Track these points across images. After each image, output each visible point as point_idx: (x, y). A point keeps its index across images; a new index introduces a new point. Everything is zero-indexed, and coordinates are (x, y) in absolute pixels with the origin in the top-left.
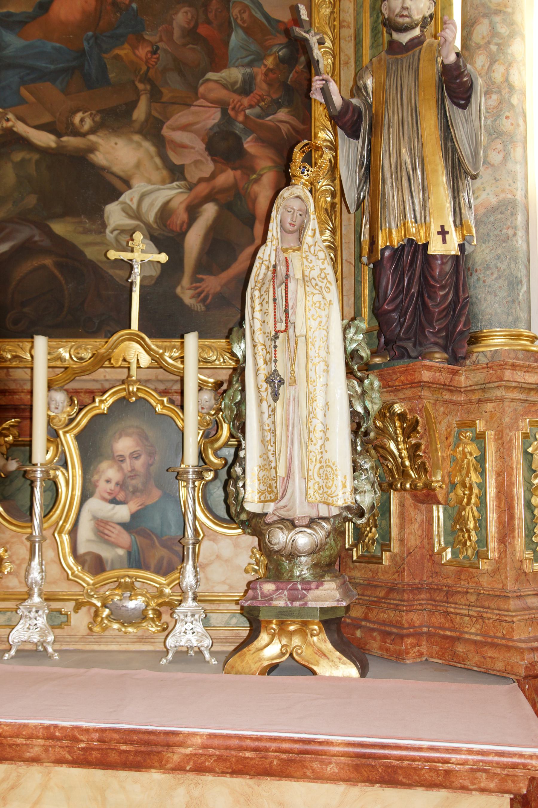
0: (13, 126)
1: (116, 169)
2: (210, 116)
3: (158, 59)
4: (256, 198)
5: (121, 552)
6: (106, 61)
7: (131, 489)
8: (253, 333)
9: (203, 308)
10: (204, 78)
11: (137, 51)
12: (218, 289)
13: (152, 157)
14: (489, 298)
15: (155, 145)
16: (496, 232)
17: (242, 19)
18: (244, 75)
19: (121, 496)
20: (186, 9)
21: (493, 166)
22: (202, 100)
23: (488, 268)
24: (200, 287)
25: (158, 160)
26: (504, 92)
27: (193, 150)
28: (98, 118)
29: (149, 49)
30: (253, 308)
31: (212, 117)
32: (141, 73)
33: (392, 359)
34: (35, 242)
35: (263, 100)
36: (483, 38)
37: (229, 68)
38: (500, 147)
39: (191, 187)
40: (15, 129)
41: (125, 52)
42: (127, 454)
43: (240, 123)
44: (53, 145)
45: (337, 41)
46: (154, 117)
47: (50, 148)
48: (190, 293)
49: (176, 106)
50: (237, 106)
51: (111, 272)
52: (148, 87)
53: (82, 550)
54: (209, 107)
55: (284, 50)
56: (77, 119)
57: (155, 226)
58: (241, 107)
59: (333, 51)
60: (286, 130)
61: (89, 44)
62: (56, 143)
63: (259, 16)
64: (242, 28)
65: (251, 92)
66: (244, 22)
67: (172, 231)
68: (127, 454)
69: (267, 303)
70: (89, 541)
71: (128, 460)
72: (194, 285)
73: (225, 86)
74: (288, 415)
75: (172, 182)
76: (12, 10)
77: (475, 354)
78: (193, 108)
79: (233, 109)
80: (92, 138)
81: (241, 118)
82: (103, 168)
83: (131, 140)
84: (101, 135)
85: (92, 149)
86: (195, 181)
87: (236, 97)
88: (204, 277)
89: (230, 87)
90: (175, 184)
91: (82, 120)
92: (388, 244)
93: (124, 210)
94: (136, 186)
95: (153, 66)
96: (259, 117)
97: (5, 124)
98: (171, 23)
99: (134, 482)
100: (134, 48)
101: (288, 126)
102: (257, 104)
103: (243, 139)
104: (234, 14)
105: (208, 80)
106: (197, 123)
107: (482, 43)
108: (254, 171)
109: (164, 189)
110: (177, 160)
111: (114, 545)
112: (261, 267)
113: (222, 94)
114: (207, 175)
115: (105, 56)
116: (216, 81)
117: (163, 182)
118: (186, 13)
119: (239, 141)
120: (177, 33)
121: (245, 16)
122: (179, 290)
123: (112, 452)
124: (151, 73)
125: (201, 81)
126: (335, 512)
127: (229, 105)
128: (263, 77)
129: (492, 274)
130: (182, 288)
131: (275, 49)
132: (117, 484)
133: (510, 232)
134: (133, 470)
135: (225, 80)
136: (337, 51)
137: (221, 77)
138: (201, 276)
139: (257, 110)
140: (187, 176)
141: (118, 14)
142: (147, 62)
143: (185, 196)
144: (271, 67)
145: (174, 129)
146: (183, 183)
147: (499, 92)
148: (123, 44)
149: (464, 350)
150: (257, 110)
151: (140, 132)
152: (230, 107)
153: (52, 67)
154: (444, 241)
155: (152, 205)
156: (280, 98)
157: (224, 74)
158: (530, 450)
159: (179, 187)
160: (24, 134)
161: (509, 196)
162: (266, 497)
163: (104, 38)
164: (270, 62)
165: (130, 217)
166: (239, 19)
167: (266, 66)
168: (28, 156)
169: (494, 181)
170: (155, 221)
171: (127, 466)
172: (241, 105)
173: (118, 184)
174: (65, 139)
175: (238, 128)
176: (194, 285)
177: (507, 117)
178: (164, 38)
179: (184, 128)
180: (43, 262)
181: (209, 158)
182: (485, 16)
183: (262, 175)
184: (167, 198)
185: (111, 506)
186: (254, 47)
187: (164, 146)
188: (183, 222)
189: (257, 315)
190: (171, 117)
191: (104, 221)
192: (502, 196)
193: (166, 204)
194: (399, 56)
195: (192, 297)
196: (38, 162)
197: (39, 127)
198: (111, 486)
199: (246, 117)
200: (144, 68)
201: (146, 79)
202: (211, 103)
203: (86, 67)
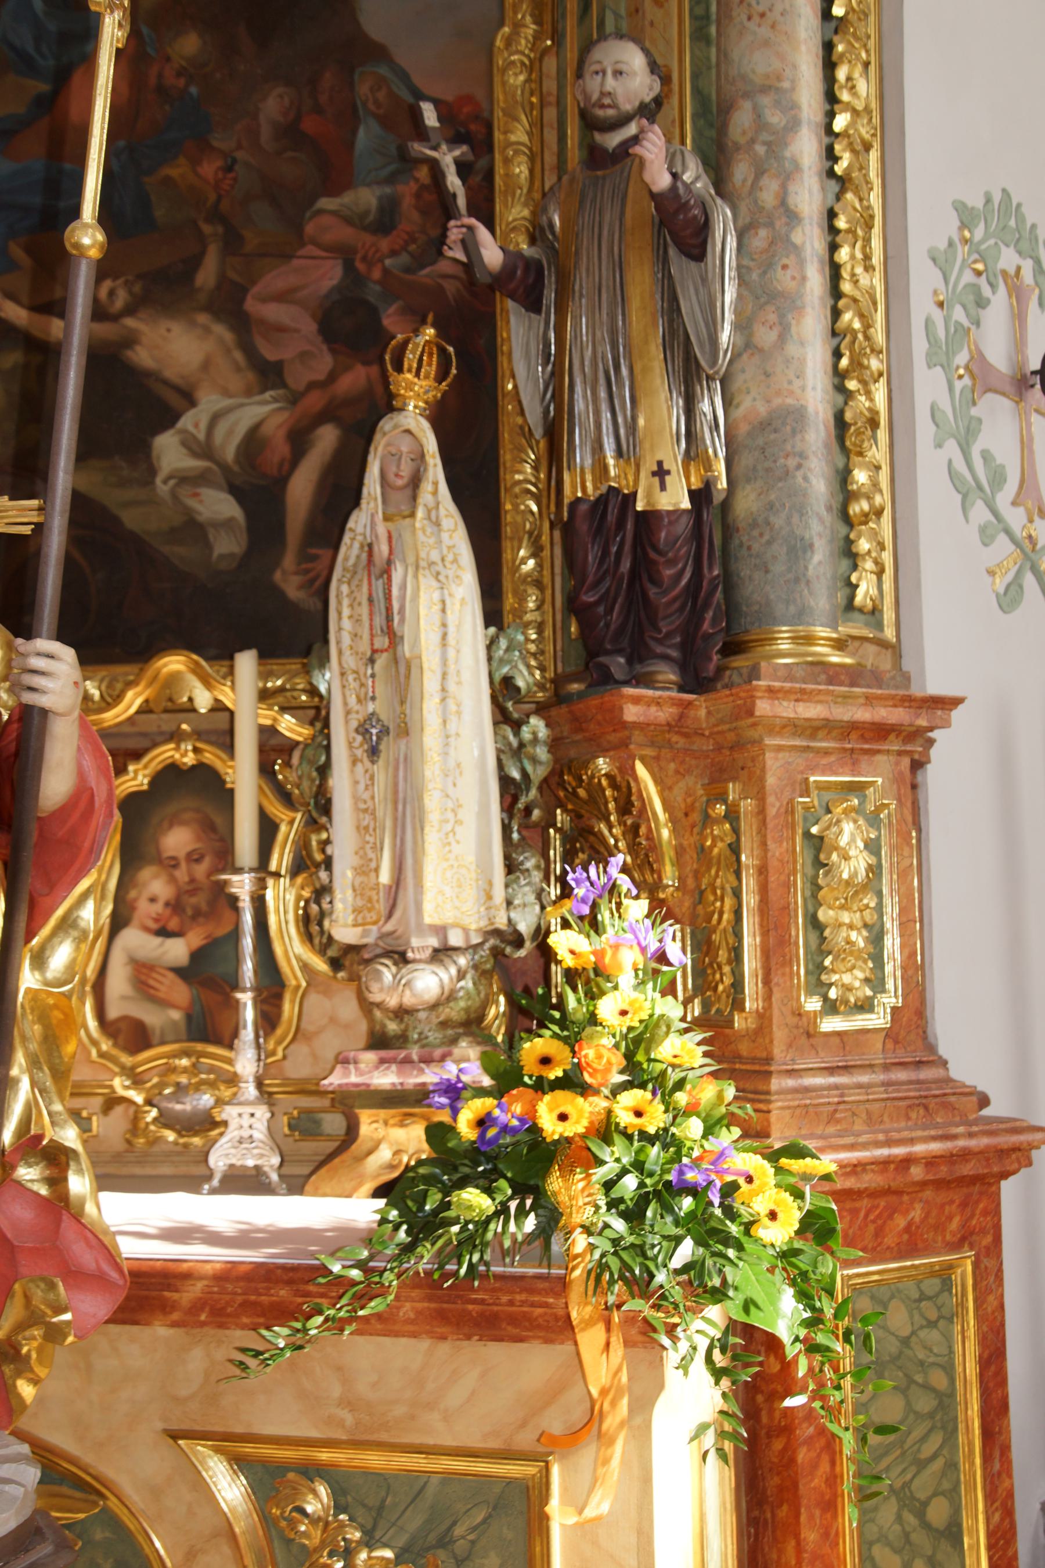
1: (169, 374)
3: (235, 179)
5: (176, 1015)
7: (189, 912)
8: (340, 653)
13: (228, 351)
14: (758, 575)
15: (233, 328)
16: (767, 464)
17: (376, 102)
18: (380, 199)
19: (173, 924)
20: (280, 90)
21: (761, 350)
23: (754, 525)
25: (238, 356)
26: (778, 224)
28: (137, 288)
29: (219, 163)
30: (339, 613)
33: (590, 686)
35: (414, 240)
36: (744, 133)
38: (772, 317)
39: (294, 399)
42: (181, 854)
51: (166, 549)
52: (220, 229)
53: (113, 1012)
54: (322, 258)
57: (236, 468)
58: (378, 255)
59: (530, 149)
68: (181, 854)
69: (360, 604)
70: (124, 998)
71: (183, 865)
72: (304, 566)
73: (348, 221)
74: (396, 785)
75: (262, 391)
77: (728, 673)
78: (295, 262)
79: (364, 259)
80: (129, 322)
81: (377, 274)
82: (148, 374)
85: (130, 341)
86: (301, 386)
87: (368, 238)
90: (267, 395)
91: (112, 293)
92: (579, 494)
93: (184, 444)
96: (408, 270)
99: (193, 900)
102: (404, 248)
105: (321, 212)
107: (742, 140)
110: (270, 353)
111: (164, 1003)
112: (351, 545)
113: (345, 234)
114: (321, 376)
117: (249, 393)
119: (374, 314)
121: (381, 95)
122: (278, 576)
123: (159, 852)
125: (308, 214)
126: (476, 940)
129: (761, 535)
132: (167, 904)
133: (792, 463)
134: (192, 880)
138: (314, 551)
139: (404, 259)
140: (290, 381)
141: (167, 107)
143: (285, 415)
145: (264, 300)
146: (281, 392)
147: (770, 225)
149: (712, 667)
152: (359, 256)
154: (663, 487)
155: (230, 432)
157: (347, 198)
158: (814, 830)
159: (275, 400)
161: (790, 401)
162: (364, 918)
165: (195, 454)
167: (417, 180)
169: (763, 377)
171: (182, 874)
173: (174, 400)
175: (373, 292)
176: (304, 566)
177: (785, 267)
179: (281, 297)
181: (324, 347)
182: (746, 95)
184: (256, 420)
185: (158, 940)
189: (346, 624)
192: (777, 401)
194: (599, 173)
195: (301, 587)
198: (158, 908)
199: (386, 271)
200: (212, 197)
201: (215, 215)
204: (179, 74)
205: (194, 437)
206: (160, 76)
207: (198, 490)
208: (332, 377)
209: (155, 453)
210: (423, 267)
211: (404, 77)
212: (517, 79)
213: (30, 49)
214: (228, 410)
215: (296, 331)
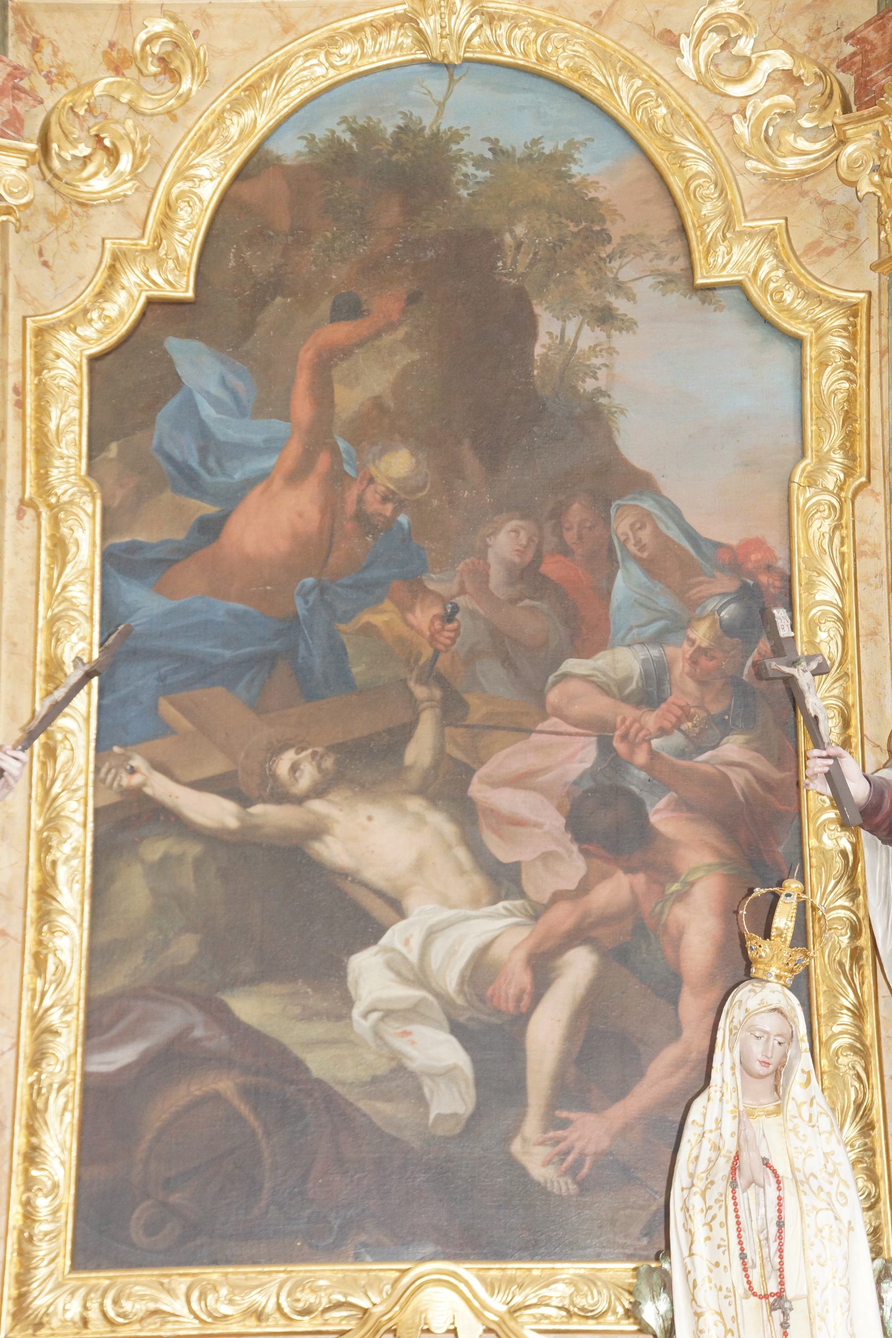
0: (144, 784)
1: (371, 875)
2: (573, 756)
3: (457, 631)
4: (681, 935)
6: (344, 638)
9: (573, 1188)
10: (559, 672)
11: (410, 617)
12: (605, 1144)
13: (449, 847)
15: (454, 819)
17: (638, 542)
18: (644, 662)
20: (514, 523)
22: (555, 720)
24: (565, 1139)
25: (462, 854)
27: (537, 830)
28: (328, 763)
29: (437, 610)
31: (578, 757)
32: (422, 662)
34: (197, 1041)
35: (689, 717)
37: (613, 647)
39: (536, 913)
40: (148, 790)
41: (385, 617)
43: (641, 768)
44: (232, 823)
45: (849, 588)
46: (451, 758)
47: (231, 832)
48: (542, 1152)
49: (500, 734)
50: (633, 731)
51: (362, 1105)
52: (438, 693)
54: (570, 734)
55: (732, 606)
56: (283, 765)
57: (460, 1001)
58: (641, 735)
59: (842, 610)
60: (742, 783)
61: (306, 602)
62: (240, 819)
63: (674, 533)
64: (638, 560)
65: (664, 700)
66: (642, 548)
67: (498, 1012)
72: (551, 1134)
73: (603, 689)
75: (494, 902)
76: (142, 537)
78: (535, 737)
79: (624, 737)
80: (317, 806)
81: (641, 757)
82: (344, 874)
83: (402, 810)
84: (337, 799)
86: (545, 898)
87: (629, 712)
88: (572, 1116)
89: (615, 690)
90: (501, 905)
91: (294, 768)
93: (390, 966)
94: (416, 912)
95: (446, 646)
96: (682, 754)
97: (127, 781)
98: (483, 553)
100: (405, 609)
101: (747, 774)
102: (677, 726)
103: (648, 803)
104: (620, 531)
105: (566, 676)
106: (545, 770)
108: (674, 876)
109: (478, 917)
110: (503, 853)
114: (571, 884)
115: (342, 627)
116: (585, 678)
117: (475, 903)
118: (516, 531)
120: (496, 576)
121: (645, 535)
122: (516, 1147)
124: (443, 663)
125: (551, 679)
127: (614, 729)
128: (687, 668)
130: (525, 1140)
131: (712, 605)
135: (605, 674)
136: (850, 608)
137: (594, 669)
138: (564, 1114)
139: (677, 739)
141: (369, 539)
142: (432, 639)
143: (524, 933)
144: (705, 644)
145: (496, 784)
146: (519, 903)
148: (380, 600)
150: (677, 739)
151: (421, 791)
152: (617, 733)
153: (228, 654)
155: (451, 953)
156: (726, 712)
159: (512, 914)
160: (168, 801)
163: (339, 589)
164: (701, 633)
165: (406, 981)
166: (632, 541)
167: (693, 642)
168: (176, 850)
170: (461, 991)
172: (641, 728)
173: (378, 909)
174: (258, 809)
178: (468, 586)
179: (519, 781)
180: (214, 1086)
181: (575, 848)
183: (692, 884)
184: (486, 938)
186: (665, 601)
187: (475, 822)
188: (522, 991)
190: (490, 755)
191: (347, 991)
193: (484, 950)
195: (547, 1163)
196: (198, 864)
197: (200, 785)
199: (653, 755)
202: (576, 726)
203: (302, 651)
204: (385, 499)
205: (405, 958)
206: (360, 500)
207: (409, 1028)
208: (584, 888)
209: (350, 978)
210: (701, 750)
211: (676, 515)
212: (821, 526)
213: (194, 462)
214: (450, 924)
215: (537, 825)
